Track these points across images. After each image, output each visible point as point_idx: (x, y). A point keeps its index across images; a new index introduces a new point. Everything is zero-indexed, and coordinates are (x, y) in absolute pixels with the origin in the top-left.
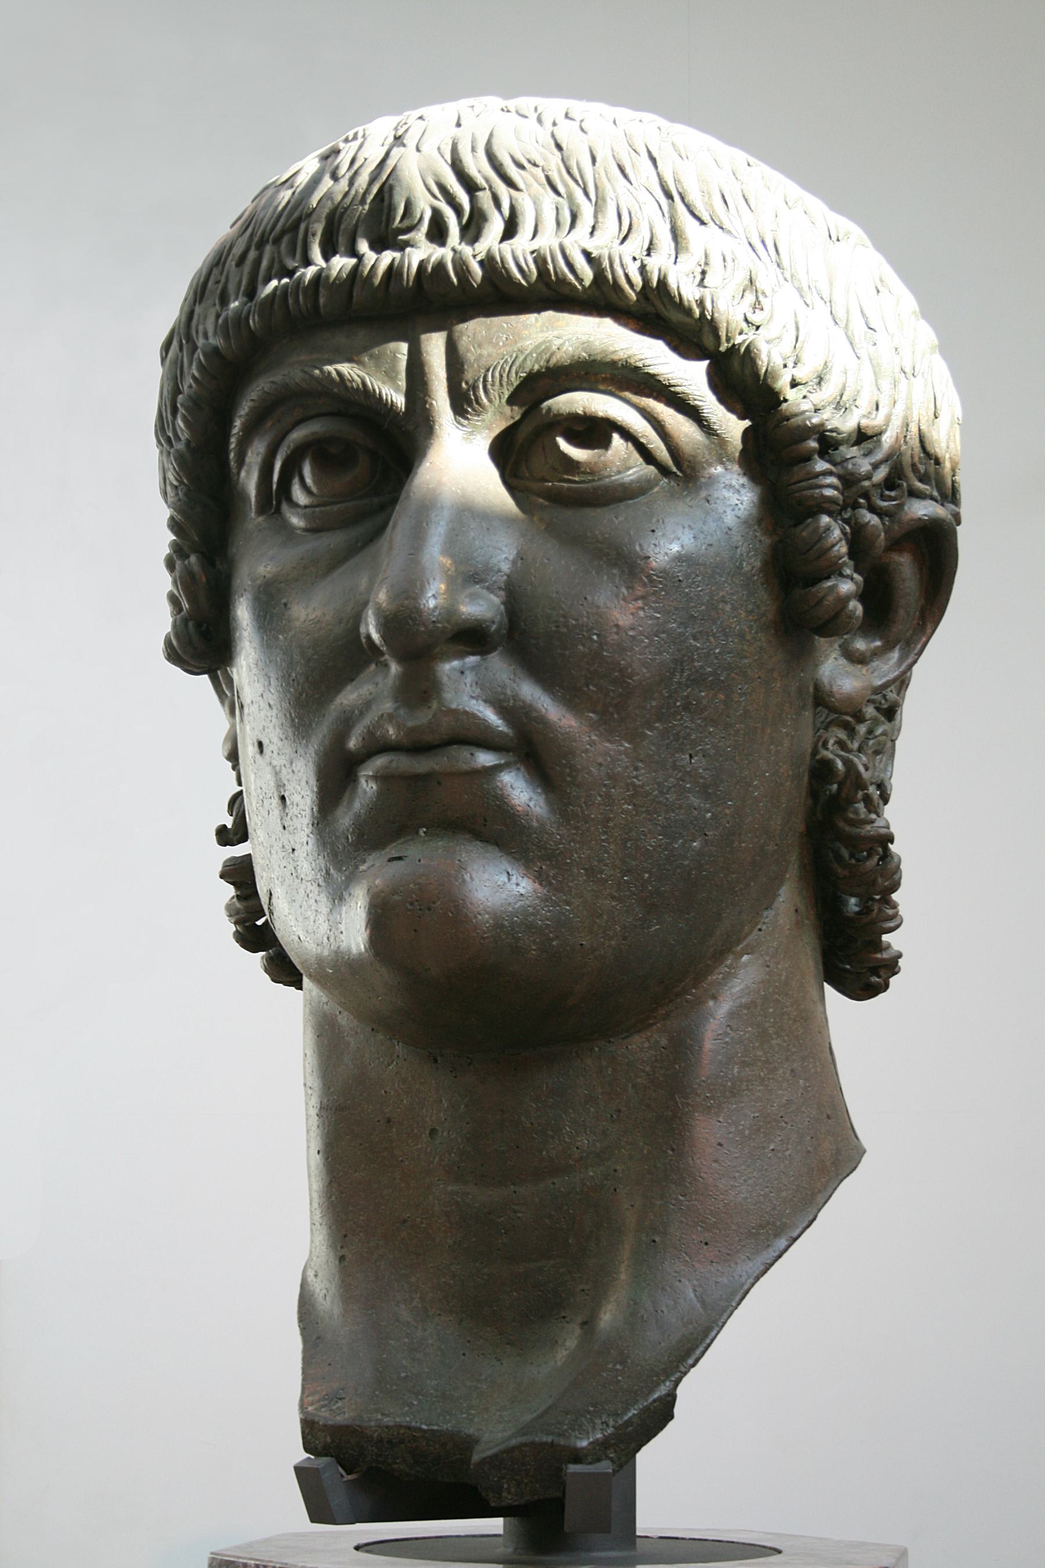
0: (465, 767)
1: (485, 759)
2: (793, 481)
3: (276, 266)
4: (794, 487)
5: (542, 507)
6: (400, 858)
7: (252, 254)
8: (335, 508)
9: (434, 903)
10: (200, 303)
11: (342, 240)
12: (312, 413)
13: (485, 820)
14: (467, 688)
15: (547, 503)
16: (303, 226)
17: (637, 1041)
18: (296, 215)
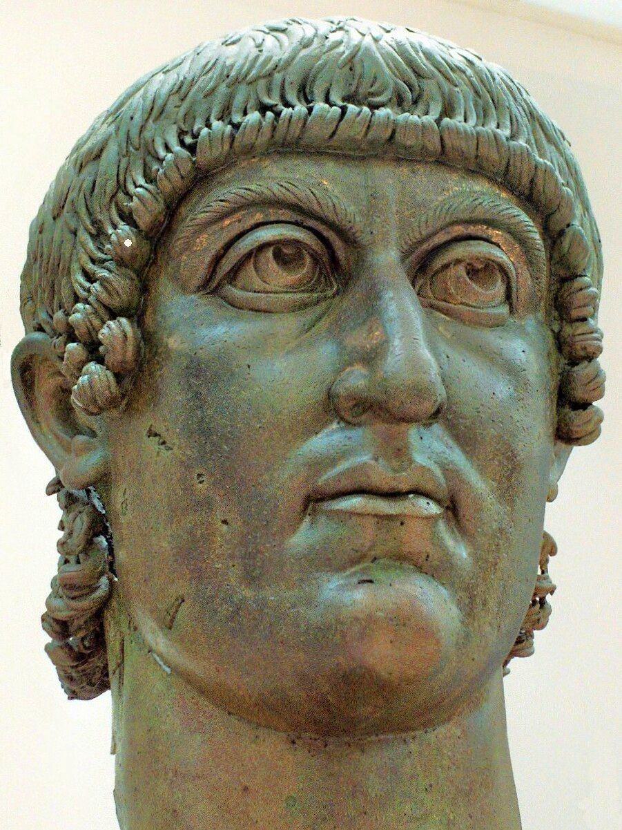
0: (426, 513)
1: (434, 509)
2: (578, 332)
3: (251, 103)
4: (581, 337)
5: (445, 321)
6: (371, 581)
7: (223, 89)
8: (289, 296)
9: (409, 620)
10: (157, 118)
11: (318, 92)
12: (272, 219)
13: (428, 556)
14: (430, 449)
15: (449, 319)
16: (278, 77)
17: (442, 730)
18: (270, 66)
